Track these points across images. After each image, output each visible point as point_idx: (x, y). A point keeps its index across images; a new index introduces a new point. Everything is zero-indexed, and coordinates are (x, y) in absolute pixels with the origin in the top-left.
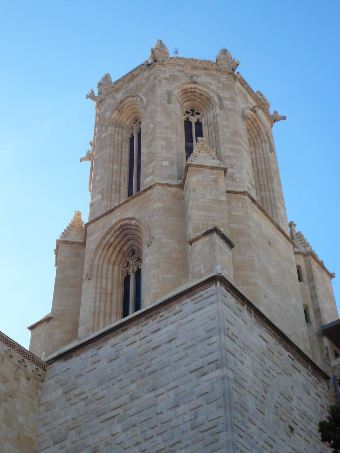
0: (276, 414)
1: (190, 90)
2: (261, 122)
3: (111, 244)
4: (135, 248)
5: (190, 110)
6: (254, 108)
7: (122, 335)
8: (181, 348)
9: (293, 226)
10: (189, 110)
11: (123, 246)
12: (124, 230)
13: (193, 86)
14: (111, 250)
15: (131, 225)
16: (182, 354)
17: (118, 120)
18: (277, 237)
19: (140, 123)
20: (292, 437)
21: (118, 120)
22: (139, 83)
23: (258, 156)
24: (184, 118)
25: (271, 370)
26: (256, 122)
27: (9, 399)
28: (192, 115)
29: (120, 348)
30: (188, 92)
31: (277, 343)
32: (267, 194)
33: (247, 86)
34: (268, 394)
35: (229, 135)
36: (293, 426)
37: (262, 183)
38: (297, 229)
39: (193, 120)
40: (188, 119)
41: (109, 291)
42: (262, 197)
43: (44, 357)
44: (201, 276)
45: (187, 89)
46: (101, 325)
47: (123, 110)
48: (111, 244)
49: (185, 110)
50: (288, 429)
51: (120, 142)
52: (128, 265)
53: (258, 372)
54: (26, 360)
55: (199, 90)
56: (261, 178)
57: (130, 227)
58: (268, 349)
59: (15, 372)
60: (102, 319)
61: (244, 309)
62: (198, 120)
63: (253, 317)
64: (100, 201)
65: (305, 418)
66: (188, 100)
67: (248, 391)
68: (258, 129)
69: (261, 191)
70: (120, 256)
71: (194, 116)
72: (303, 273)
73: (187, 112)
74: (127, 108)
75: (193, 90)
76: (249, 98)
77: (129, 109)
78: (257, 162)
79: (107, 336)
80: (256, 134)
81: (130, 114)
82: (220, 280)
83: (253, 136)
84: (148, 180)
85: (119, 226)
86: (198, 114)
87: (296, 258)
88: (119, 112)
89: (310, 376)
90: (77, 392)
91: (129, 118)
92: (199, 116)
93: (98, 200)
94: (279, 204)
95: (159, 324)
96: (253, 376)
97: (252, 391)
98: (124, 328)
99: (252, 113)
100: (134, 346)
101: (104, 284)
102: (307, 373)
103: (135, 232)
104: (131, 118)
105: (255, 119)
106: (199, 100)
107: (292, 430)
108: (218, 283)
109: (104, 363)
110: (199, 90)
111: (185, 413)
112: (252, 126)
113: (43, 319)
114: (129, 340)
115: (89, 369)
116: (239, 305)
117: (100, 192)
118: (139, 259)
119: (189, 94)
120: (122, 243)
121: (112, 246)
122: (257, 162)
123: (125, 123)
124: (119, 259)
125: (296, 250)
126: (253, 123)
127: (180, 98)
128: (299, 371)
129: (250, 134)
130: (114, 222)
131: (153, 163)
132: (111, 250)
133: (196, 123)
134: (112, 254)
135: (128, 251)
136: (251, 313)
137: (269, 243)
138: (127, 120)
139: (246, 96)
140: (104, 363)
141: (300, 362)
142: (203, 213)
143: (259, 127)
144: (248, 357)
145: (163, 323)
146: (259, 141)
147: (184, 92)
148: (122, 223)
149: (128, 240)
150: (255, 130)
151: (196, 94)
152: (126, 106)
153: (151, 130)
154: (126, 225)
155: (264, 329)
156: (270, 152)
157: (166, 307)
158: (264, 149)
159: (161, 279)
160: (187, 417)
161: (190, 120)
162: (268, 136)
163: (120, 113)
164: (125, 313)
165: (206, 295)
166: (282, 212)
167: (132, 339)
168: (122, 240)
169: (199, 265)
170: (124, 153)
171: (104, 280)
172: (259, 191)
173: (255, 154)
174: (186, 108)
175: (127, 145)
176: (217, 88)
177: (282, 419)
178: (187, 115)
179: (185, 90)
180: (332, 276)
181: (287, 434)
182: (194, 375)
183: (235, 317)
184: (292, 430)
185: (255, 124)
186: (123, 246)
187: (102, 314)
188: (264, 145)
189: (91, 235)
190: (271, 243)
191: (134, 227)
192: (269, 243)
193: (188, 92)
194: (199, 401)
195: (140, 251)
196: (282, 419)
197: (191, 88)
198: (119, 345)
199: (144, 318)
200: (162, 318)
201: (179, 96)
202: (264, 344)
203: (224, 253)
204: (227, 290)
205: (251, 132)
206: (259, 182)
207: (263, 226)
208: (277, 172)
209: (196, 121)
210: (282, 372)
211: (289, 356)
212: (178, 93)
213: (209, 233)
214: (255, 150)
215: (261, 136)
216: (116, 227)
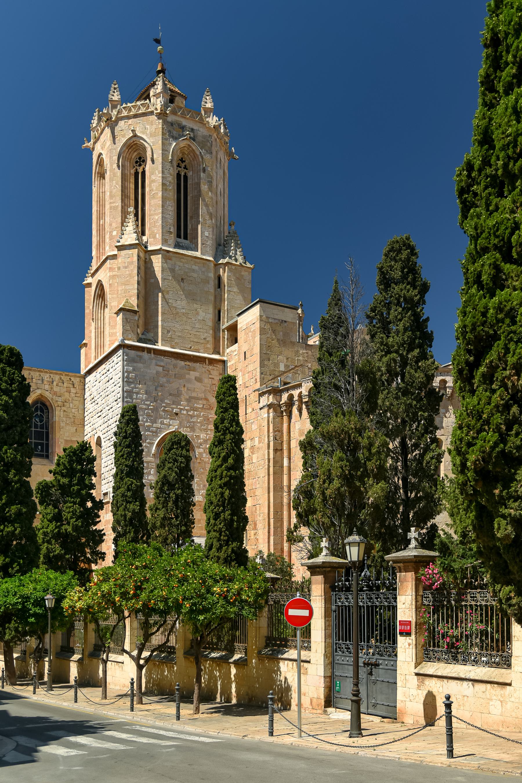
24: (133, 171)
30: (132, 146)
39: (140, 170)
40: (137, 170)
66: (135, 151)
75: (135, 142)
119: (134, 147)
133: (142, 172)
193: (132, 146)
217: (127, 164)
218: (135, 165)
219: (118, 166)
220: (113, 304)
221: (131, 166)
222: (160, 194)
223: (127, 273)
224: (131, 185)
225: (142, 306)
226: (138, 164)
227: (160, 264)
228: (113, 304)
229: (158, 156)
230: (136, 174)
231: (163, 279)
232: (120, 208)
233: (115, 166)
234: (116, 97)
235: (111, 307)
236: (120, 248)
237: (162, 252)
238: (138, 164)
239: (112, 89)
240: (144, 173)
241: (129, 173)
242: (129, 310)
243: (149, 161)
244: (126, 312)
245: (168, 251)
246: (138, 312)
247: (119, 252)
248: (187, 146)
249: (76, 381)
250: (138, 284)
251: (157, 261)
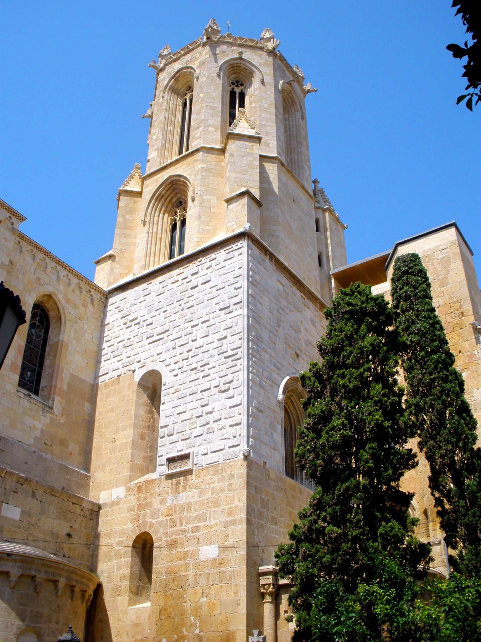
0: (286, 343)
1: (236, 65)
2: (296, 94)
3: (163, 196)
4: (182, 200)
5: (236, 82)
6: (290, 81)
7: (168, 275)
8: (214, 289)
9: (317, 183)
10: (234, 82)
11: (172, 198)
12: (173, 185)
13: (239, 61)
14: (162, 200)
15: (180, 181)
16: (214, 294)
17: (174, 87)
18: (301, 195)
19: (192, 91)
20: (297, 361)
21: (174, 87)
22: (194, 56)
23: (291, 123)
24: (230, 89)
25: (285, 309)
26: (291, 93)
27: (78, 320)
28: (237, 86)
29: (166, 285)
30: (234, 67)
31: (292, 286)
32: (296, 157)
33: (285, 62)
34: (281, 328)
35: (266, 106)
36: (298, 352)
37: (292, 146)
38: (320, 186)
39: (238, 90)
40: (233, 89)
41: (159, 236)
42: (291, 159)
43: (106, 289)
44: (233, 231)
45: (233, 64)
46: (151, 264)
47: (179, 79)
48: (163, 196)
49: (231, 81)
50: (295, 356)
51: (175, 106)
52: (176, 214)
53: (274, 310)
54: (92, 290)
55: (244, 65)
56: (292, 142)
57: (178, 183)
58: (284, 291)
59: (84, 300)
60: (152, 259)
61: (267, 259)
62: (242, 91)
63: (274, 265)
64: (156, 158)
65: (310, 345)
66: (234, 73)
67: (264, 326)
68: (293, 99)
69: (291, 153)
70: (170, 206)
71: (239, 87)
72: (320, 225)
73: (233, 84)
74: (183, 77)
75: (239, 65)
76: (287, 73)
77: (183, 78)
78: (289, 129)
79: (156, 274)
80: (291, 103)
81: (184, 82)
82: (248, 236)
84: (196, 143)
85: (169, 181)
86: (242, 85)
87: (315, 212)
88: (175, 80)
89: (317, 312)
90: (131, 318)
91: (183, 86)
92: (243, 87)
93: (154, 157)
94: (305, 166)
95: (198, 267)
96: (269, 314)
97: (267, 326)
98: (170, 268)
99: (288, 86)
100: (177, 284)
101: (155, 229)
102: (315, 309)
103: (183, 187)
104: (186, 86)
105: (290, 91)
106: (244, 74)
107: (298, 356)
108: (246, 238)
109: (154, 294)
110: (244, 65)
111: (213, 342)
112: (288, 96)
113: (52, 376)
114: (173, 279)
115: (140, 300)
116: (263, 256)
117: (156, 150)
118: (185, 210)
119: (236, 68)
120: (172, 195)
121: (164, 198)
122: (289, 129)
123: (180, 90)
124: (169, 208)
125: (317, 205)
126: (288, 94)
127: (227, 72)
128: (309, 308)
129: (286, 104)
130: (166, 177)
131: (201, 128)
132: (162, 200)
133: (239, 93)
134: (169, 196)
135: (177, 202)
136: (272, 261)
137: (294, 200)
138: (182, 87)
139: (284, 71)
140: (154, 294)
141: (310, 301)
142: (238, 175)
143: (293, 98)
144: (266, 299)
145: (200, 267)
146: (293, 109)
147: (231, 66)
148: (172, 179)
149: (177, 193)
150: (290, 100)
151: (241, 69)
152: (182, 75)
153: (201, 99)
154: (176, 180)
155: (282, 274)
156: (301, 120)
157: (204, 254)
158: (297, 117)
159: (201, 229)
160: (215, 345)
161: (235, 90)
162: (301, 106)
163: (176, 81)
164: (171, 256)
165: (237, 247)
166: (308, 172)
167: (175, 278)
168: (172, 192)
169: (232, 221)
170: (177, 116)
171: (155, 226)
172: (289, 154)
173: (289, 121)
174: (232, 80)
175: (181, 108)
176: (260, 64)
177: (290, 347)
178: (233, 86)
179: (232, 65)
180: (344, 228)
181: (293, 359)
182: (223, 312)
183: (259, 266)
184: (298, 356)
185: (291, 95)
186: (172, 198)
187: (152, 254)
188: (296, 113)
189: (147, 187)
190: (295, 200)
191: (182, 183)
192: (294, 200)
193: (234, 67)
194: (224, 334)
195: (186, 203)
196: (290, 347)
197: (237, 63)
198: (165, 282)
199: (186, 262)
200: (200, 263)
201: (226, 70)
202: (281, 287)
203: (253, 212)
204: (253, 243)
205: (287, 102)
206: (290, 146)
207: (289, 186)
208: (306, 138)
209: (240, 91)
210: (293, 309)
211: (301, 296)
212: (226, 68)
213: (242, 194)
214: (289, 118)
215: (295, 105)
216: (168, 182)
219: (219, 76)
220: (205, 197)
223: (244, 162)
228: (205, 197)
231: (280, 189)
235: (204, 200)
249: (97, 296)
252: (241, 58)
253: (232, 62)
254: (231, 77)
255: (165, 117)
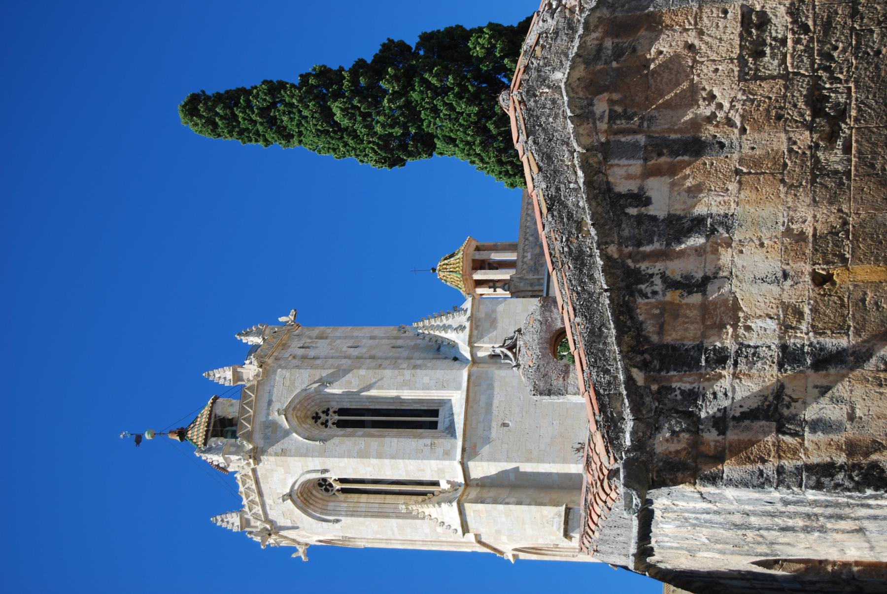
13: (295, 497)
23: (346, 400)
24: (342, 496)
30: (305, 499)
39: (338, 486)
40: (338, 490)
66: (311, 493)
75: (299, 495)
80: (310, 401)
83: (313, 404)
119: (305, 496)
142: (527, 526)
143: (300, 402)
146: (318, 397)
147: (307, 504)
179: (305, 504)
193: (305, 499)
197: (299, 498)
205: (309, 407)
217: (331, 506)
218: (331, 493)
219: (337, 521)
221: (333, 499)
222: (374, 461)
224: (362, 500)
225: (555, 495)
226: (330, 489)
227: (485, 464)
229: (315, 463)
230: (344, 491)
232: (400, 521)
233: (337, 525)
234: (232, 521)
236: (465, 529)
237: (465, 460)
238: (330, 489)
239: (224, 525)
240: (342, 481)
241: (345, 505)
242: (566, 522)
243: (324, 476)
244: (569, 528)
245: (464, 450)
246: (566, 505)
247: (471, 530)
248: (295, 412)
250: (521, 504)
251: (481, 469)
252: (290, 496)
253: (302, 505)
254: (320, 496)
255: (402, 544)
